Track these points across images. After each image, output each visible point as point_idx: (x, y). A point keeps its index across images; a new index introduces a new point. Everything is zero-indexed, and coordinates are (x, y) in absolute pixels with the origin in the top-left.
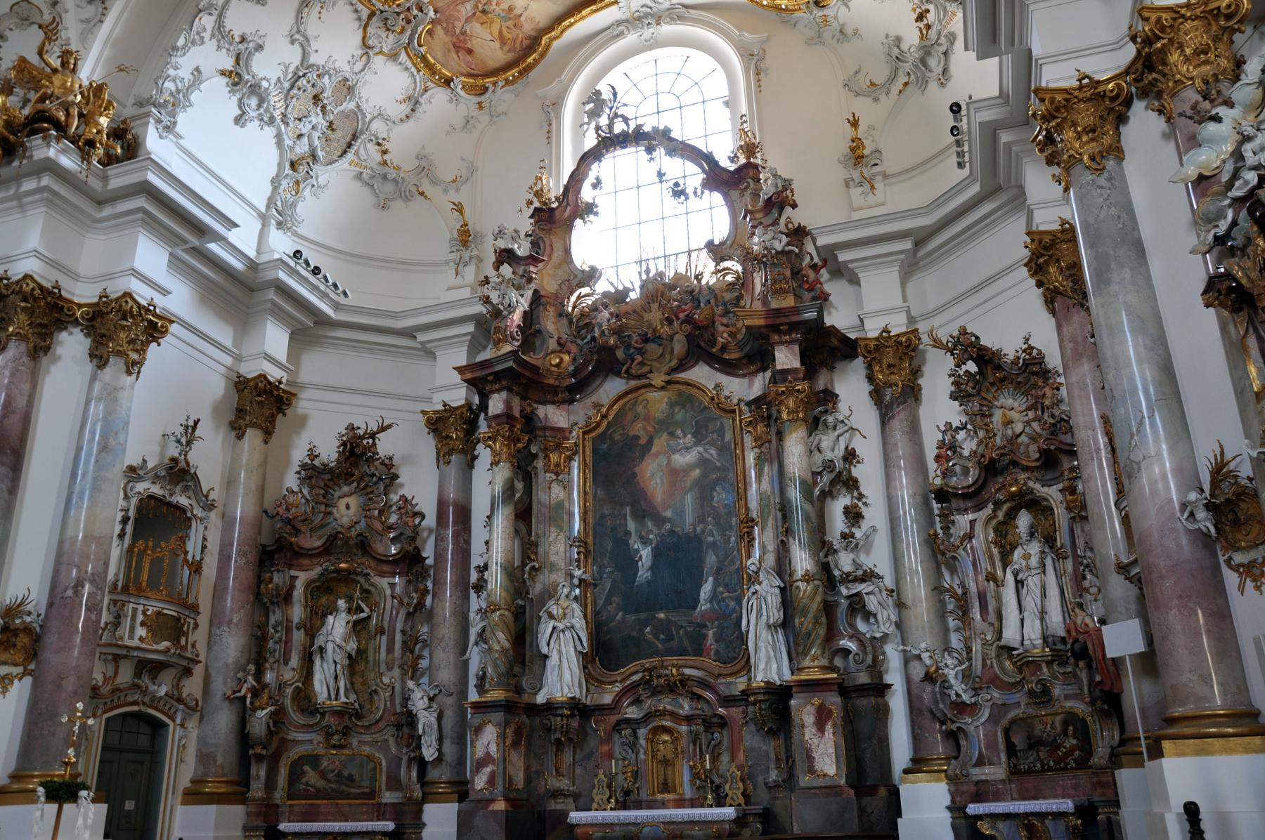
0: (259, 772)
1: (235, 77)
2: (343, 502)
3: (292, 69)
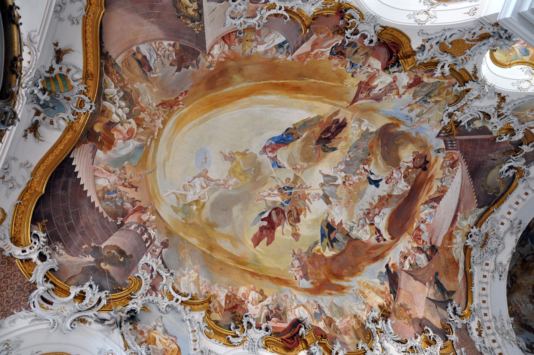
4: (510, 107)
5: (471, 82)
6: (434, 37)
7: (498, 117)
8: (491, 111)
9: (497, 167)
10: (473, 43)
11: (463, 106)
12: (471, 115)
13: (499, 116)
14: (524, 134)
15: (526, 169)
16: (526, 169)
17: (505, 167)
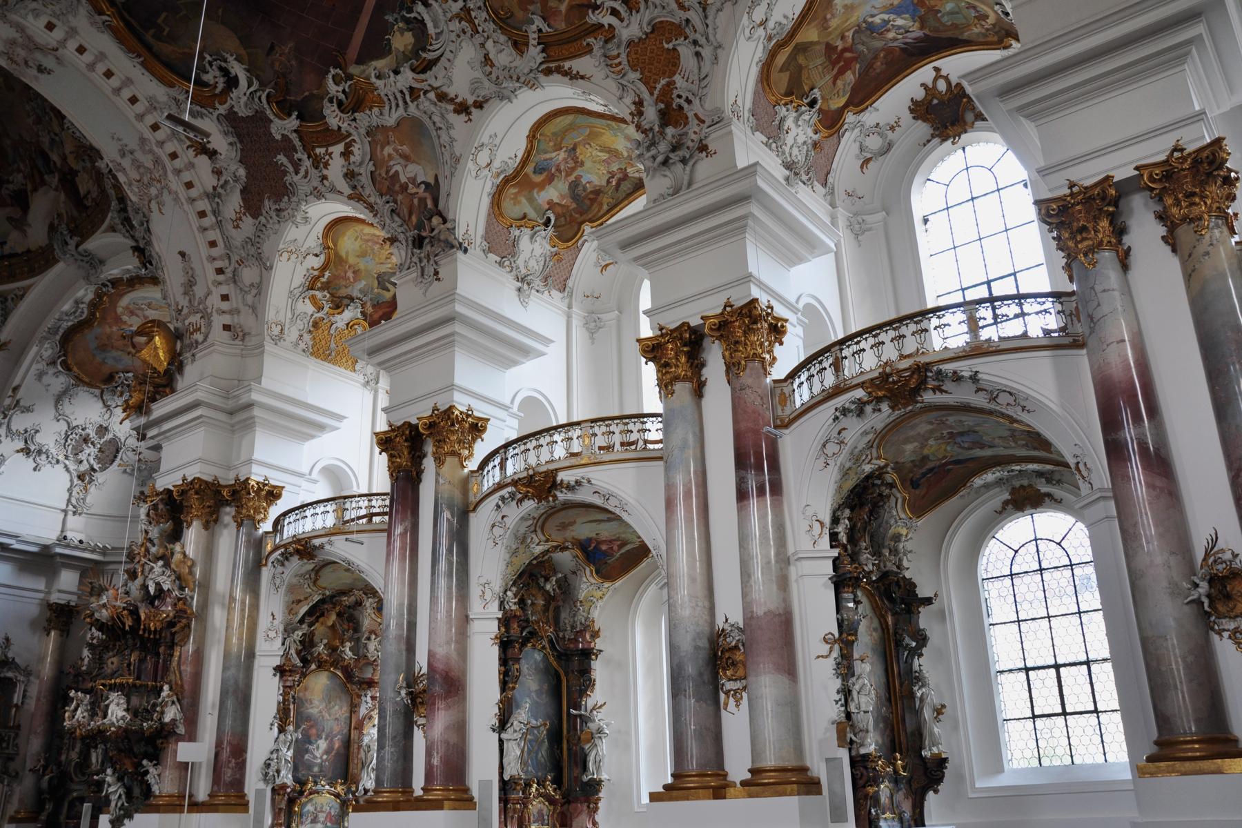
0: (49, 807)
1: (26, 451)
2: (109, 662)
3: (63, 433)
4: (436, 119)
5: (540, 59)
6: (708, 22)
7: (411, 87)
8: (435, 78)
9: (243, 52)
10: (656, 92)
11: (471, 21)
12: (442, 32)
13: (411, 89)
14: (336, 128)
15: (217, 112)
16: (217, 112)
17: (238, 70)
